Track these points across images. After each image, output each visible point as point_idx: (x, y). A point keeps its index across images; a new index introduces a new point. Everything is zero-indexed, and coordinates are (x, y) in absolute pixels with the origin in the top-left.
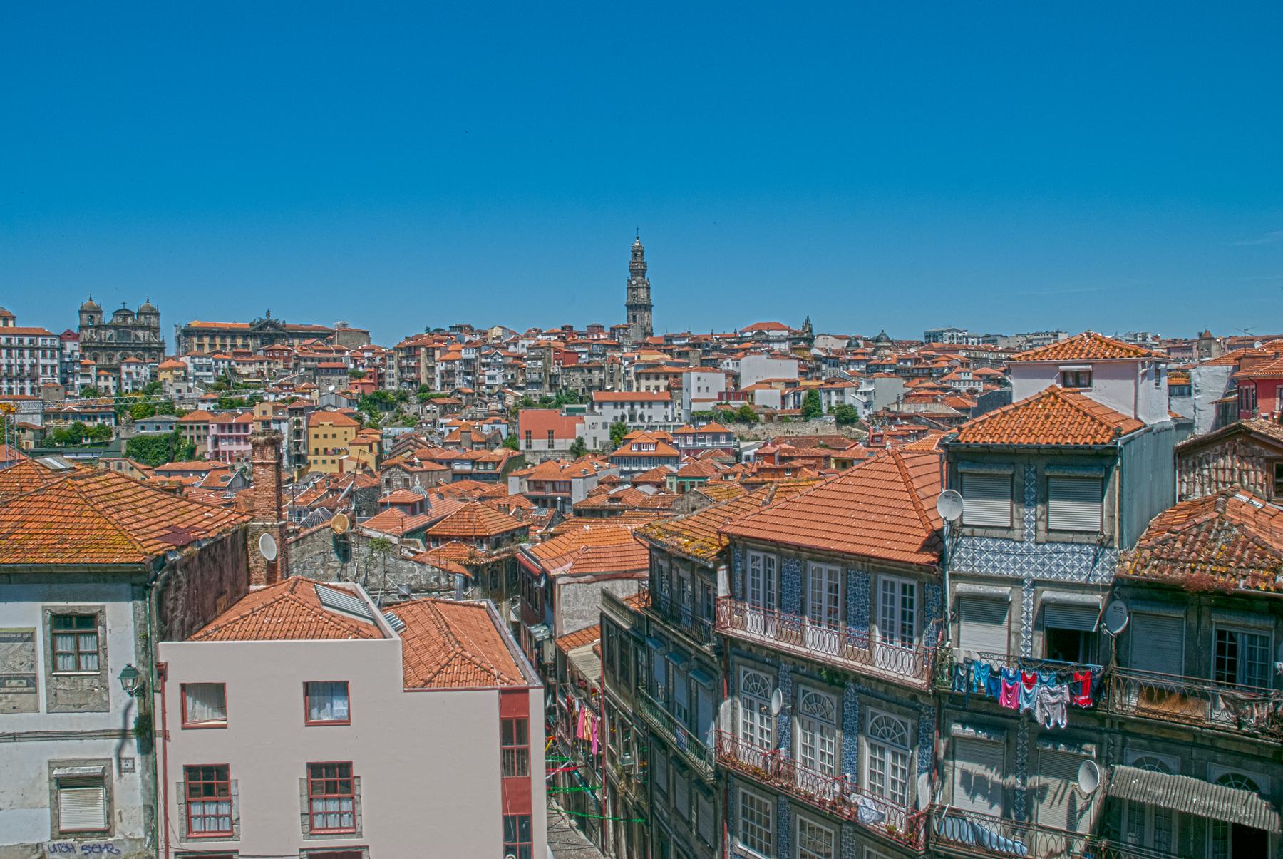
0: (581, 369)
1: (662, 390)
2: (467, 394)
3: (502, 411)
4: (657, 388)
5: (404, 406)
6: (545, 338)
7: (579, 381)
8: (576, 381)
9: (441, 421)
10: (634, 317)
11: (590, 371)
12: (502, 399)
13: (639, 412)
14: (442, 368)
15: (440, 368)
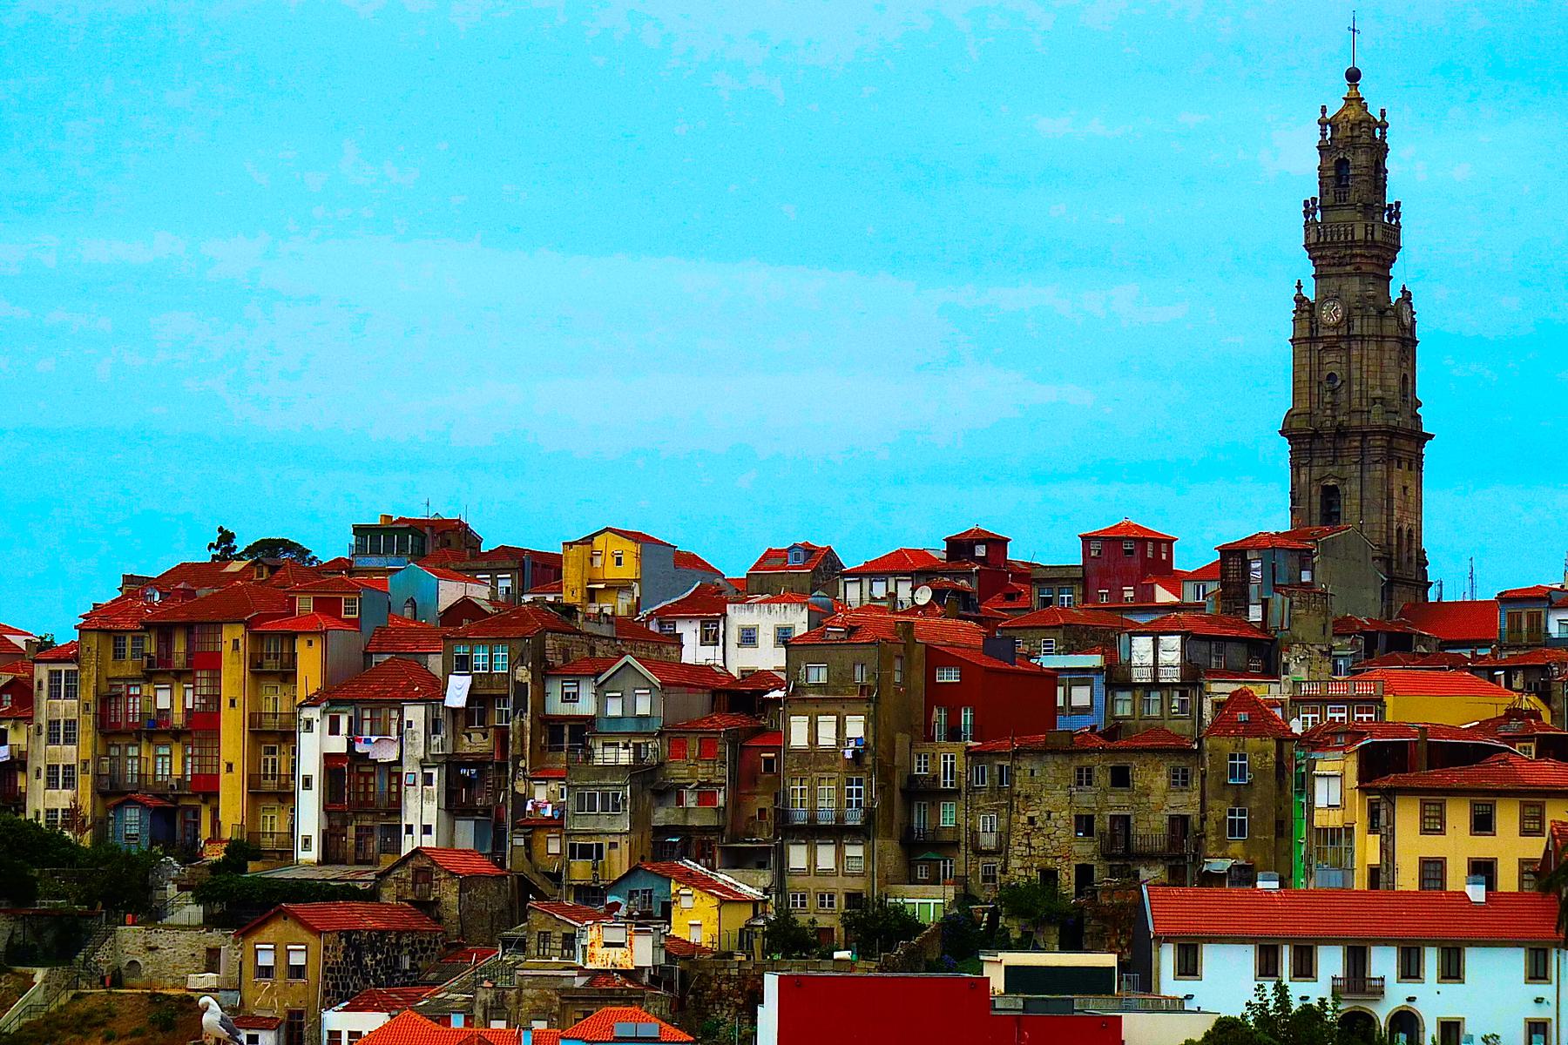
0: (1070, 747)
1: (1508, 880)
2: (467, 882)
3: (659, 976)
4: (1483, 869)
5: (130, 938)
6: (853, 593)
7: (1062, 821)
8: (1044, 823)
9: (337, 1020)
10: (1331, 496)
11: (1121, 778)
12: (652, 916)
13: (1397, 994)
14: (338, 745)
15: (315, 746)
